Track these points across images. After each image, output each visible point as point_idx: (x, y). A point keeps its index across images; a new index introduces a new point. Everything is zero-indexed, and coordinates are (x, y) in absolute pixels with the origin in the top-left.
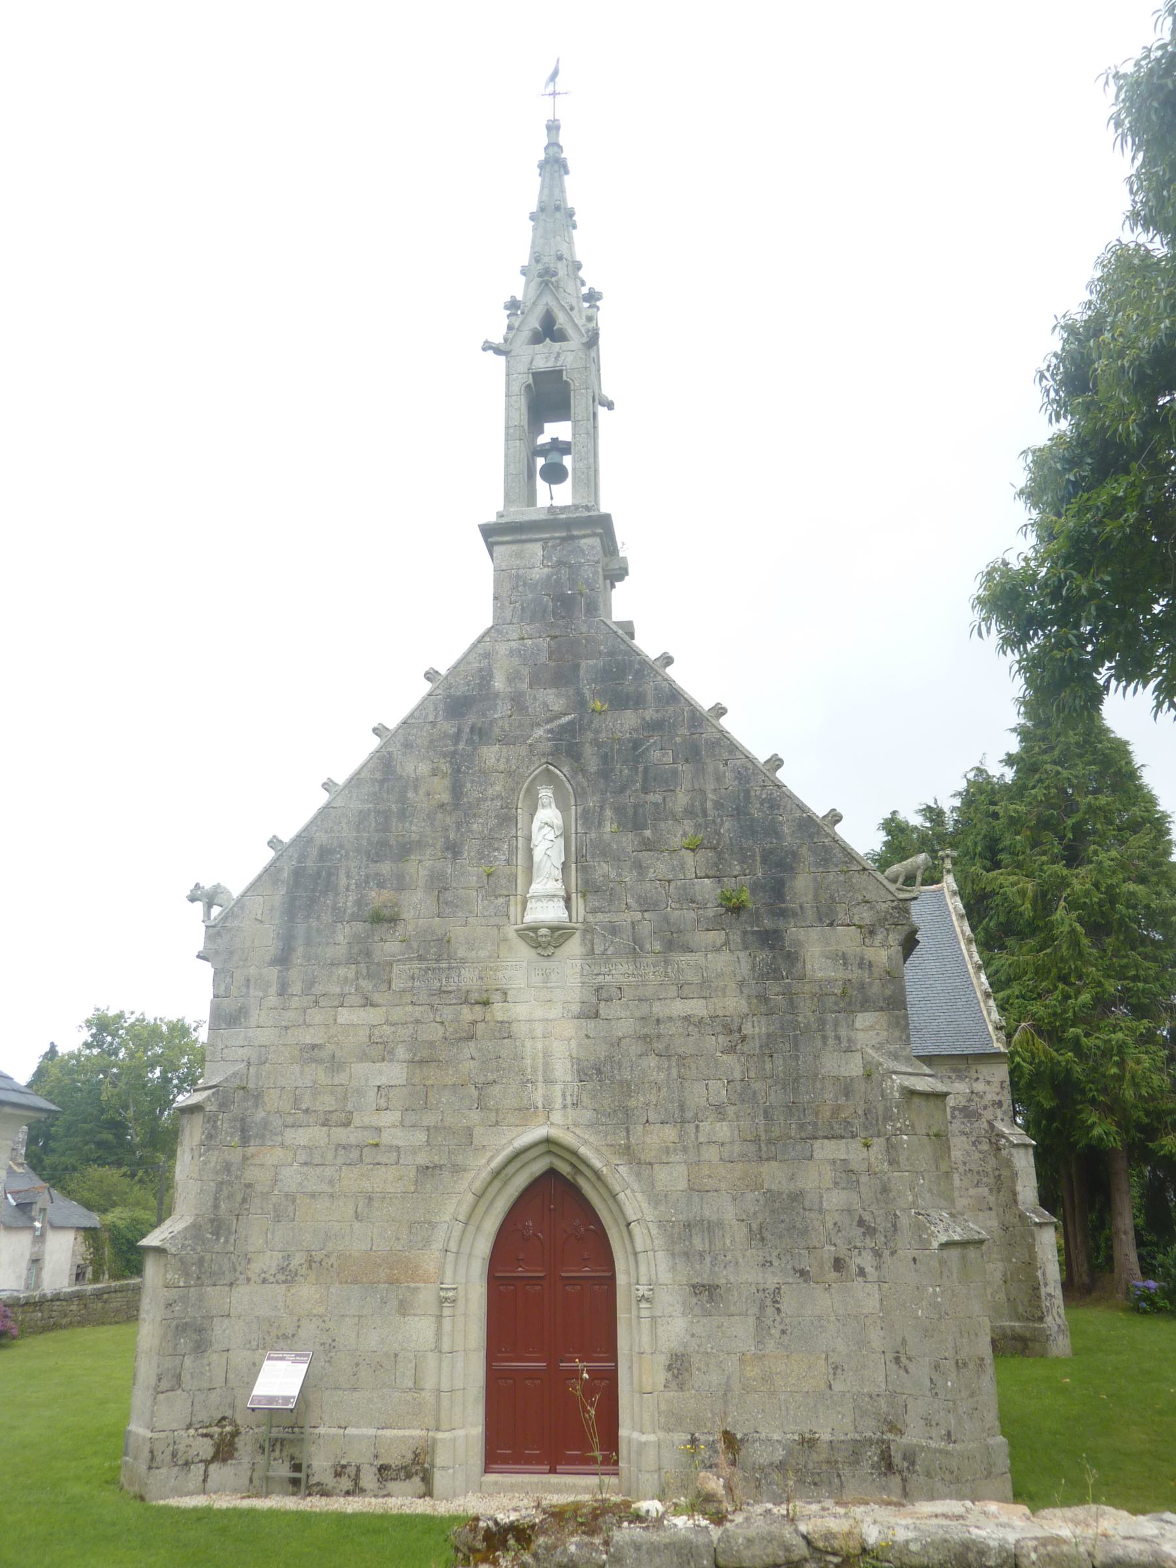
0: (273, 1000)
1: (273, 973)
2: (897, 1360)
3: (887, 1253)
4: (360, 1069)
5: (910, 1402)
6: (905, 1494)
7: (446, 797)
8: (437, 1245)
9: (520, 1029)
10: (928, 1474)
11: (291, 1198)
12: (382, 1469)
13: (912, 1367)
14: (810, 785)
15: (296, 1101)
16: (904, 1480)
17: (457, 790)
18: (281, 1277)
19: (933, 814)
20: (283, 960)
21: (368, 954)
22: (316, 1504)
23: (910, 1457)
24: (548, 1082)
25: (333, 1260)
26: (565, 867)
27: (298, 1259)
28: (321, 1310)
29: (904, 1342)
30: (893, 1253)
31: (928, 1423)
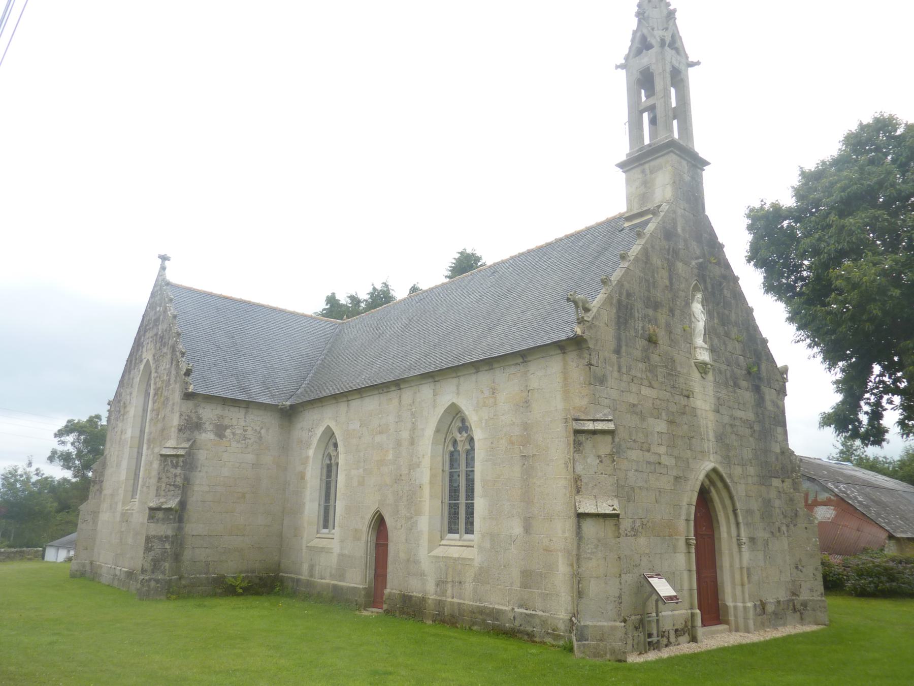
0: (616, 374)
1: (614, 357)
2: (797, 568)
3: (792, 526)
4: (651, 421)
5: (803, 584)
6: (802, 619)
7: (668, 284)
8: (683, 517)
9: (699, 412)
10: (814, 610)
11: (633, 489)
12: (676, 631)
13: (804, 570)
14: (439, 283)
15: (630, 435)
16: (801, 614)
17: (671, 284)
18: (632, 533)
19: (355, 300)
20: (617, 351)
21: (649, 359)
22: (665, 653)
23: (805, 604)
24: (708, 440)
25: (650, 524)
26: (705, 335)
27: (638, 524)
28: (647, 551)
29: (800, 560)
30: (795, 525)
31: (811, 590)
